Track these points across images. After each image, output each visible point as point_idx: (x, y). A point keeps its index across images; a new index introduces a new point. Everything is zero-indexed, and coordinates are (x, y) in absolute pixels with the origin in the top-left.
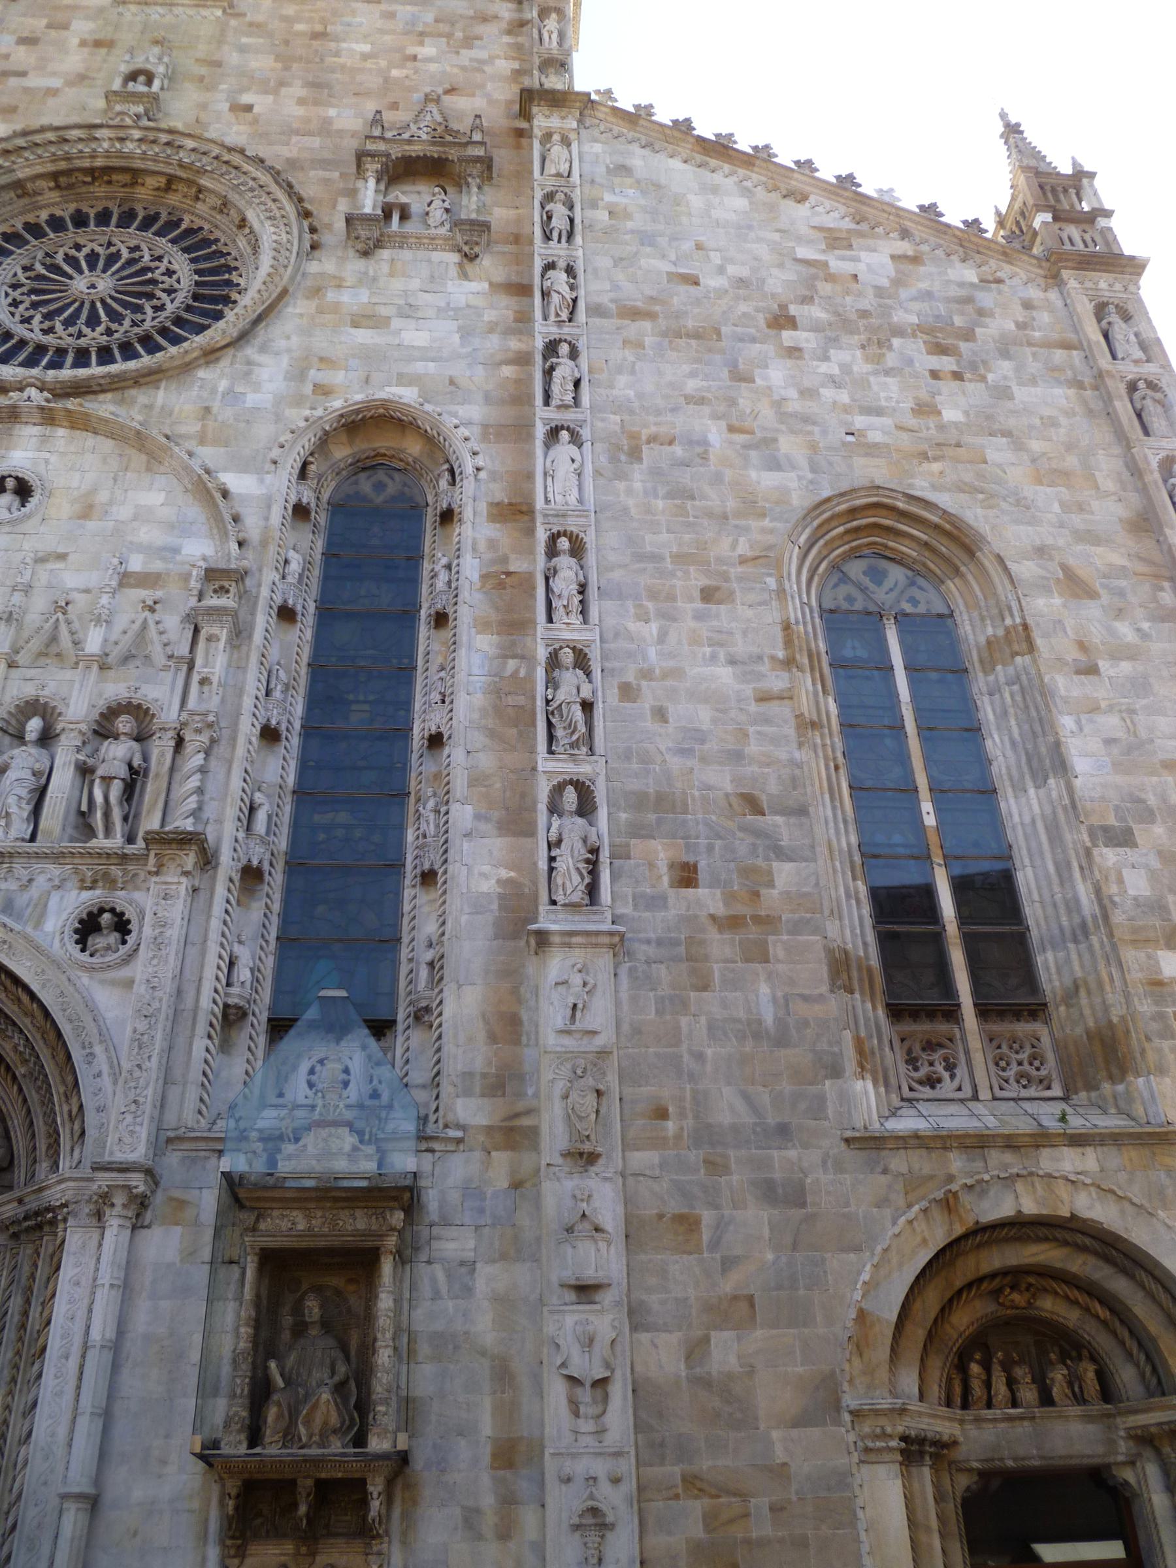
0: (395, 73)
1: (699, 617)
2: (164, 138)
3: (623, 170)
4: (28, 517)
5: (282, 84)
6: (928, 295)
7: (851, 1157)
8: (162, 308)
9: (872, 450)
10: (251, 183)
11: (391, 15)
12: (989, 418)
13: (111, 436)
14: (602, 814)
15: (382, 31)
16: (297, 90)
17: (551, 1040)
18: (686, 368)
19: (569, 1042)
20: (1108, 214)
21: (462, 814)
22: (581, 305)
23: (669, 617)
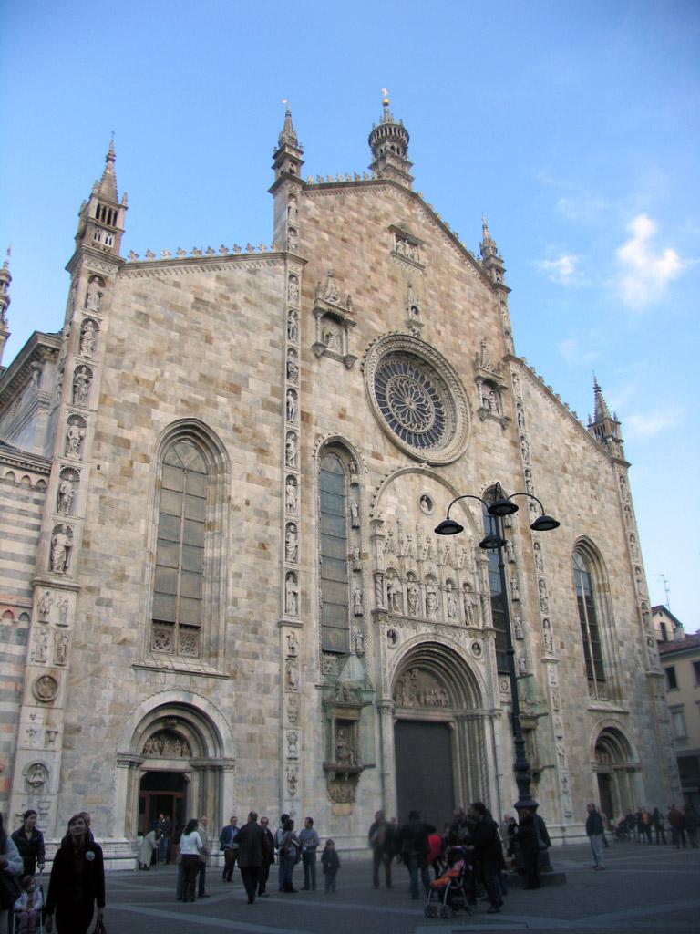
0: (471, 324)
1: (559, 572)
2: (430, 349)
3: (528, 394)
4: (434, 513)
5: (445, 322)
6: (589, 465)
7: (589, 713)
8: (428, 419)
9: (582, 522)
11: (463, 289)
12: (601, 514)
13: (444, 485)
14: (552, 628)
15: (465, 299)
16: (449, 327)
17: (550, 685)
18: (549, 485)
19: (553, 685)
20: (623, 441)
21: (528, 624)
22: (530, 457)
23: (554, 571)
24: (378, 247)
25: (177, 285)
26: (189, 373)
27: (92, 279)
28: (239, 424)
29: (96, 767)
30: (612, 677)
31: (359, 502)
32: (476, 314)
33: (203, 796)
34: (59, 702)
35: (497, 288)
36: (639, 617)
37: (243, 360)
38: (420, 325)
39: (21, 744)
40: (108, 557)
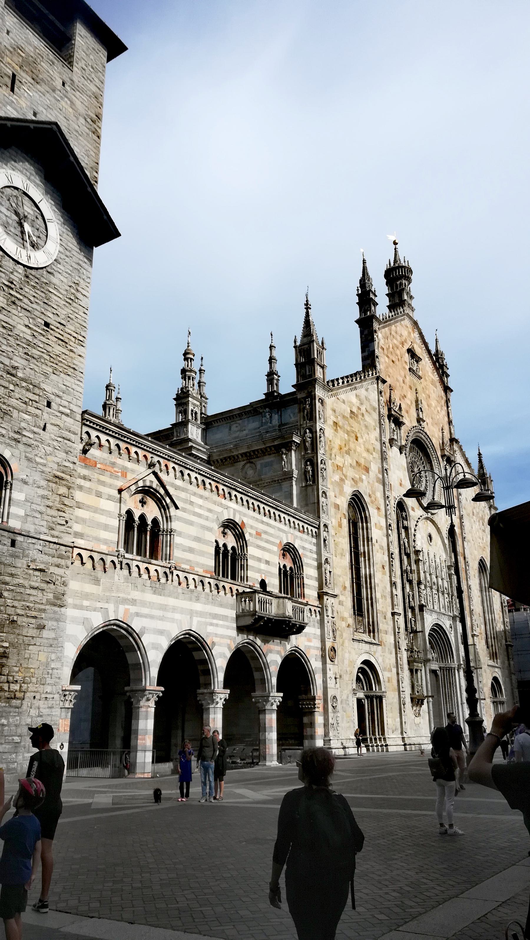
10: (434, 456)
16: (431, 420)
24: (404, 364)
25: (344, 402)
26: (353, 461)
27: (320, 399)
28: (371, 493)
29: (348, 697)
30: (492, 646)
31: (408, 539)
32: (439, 409)
33: (372, 713)
34: (336, 661)
35: (447, 389)
36: (502, 609)
37: (368, 451)
38: (424, 421)
39: (328, 686)
40: (339, 576)
